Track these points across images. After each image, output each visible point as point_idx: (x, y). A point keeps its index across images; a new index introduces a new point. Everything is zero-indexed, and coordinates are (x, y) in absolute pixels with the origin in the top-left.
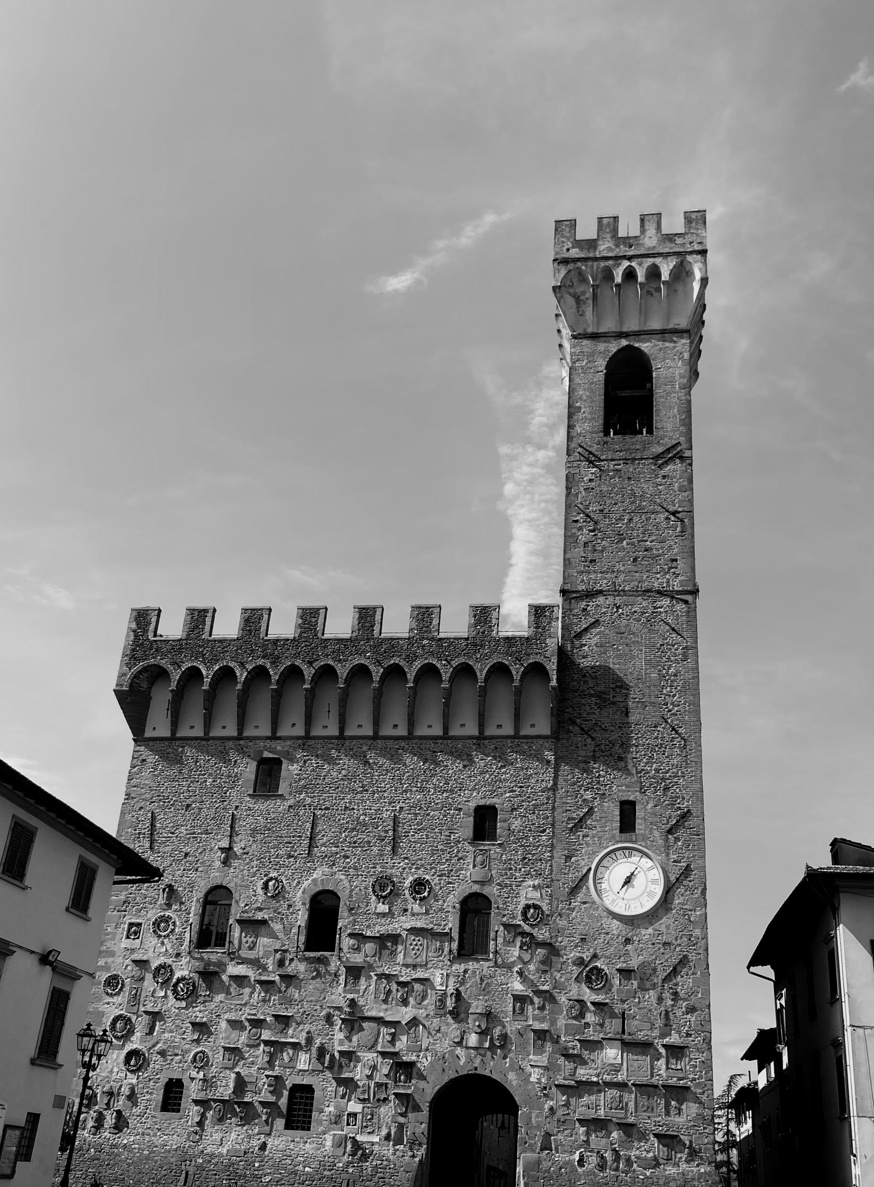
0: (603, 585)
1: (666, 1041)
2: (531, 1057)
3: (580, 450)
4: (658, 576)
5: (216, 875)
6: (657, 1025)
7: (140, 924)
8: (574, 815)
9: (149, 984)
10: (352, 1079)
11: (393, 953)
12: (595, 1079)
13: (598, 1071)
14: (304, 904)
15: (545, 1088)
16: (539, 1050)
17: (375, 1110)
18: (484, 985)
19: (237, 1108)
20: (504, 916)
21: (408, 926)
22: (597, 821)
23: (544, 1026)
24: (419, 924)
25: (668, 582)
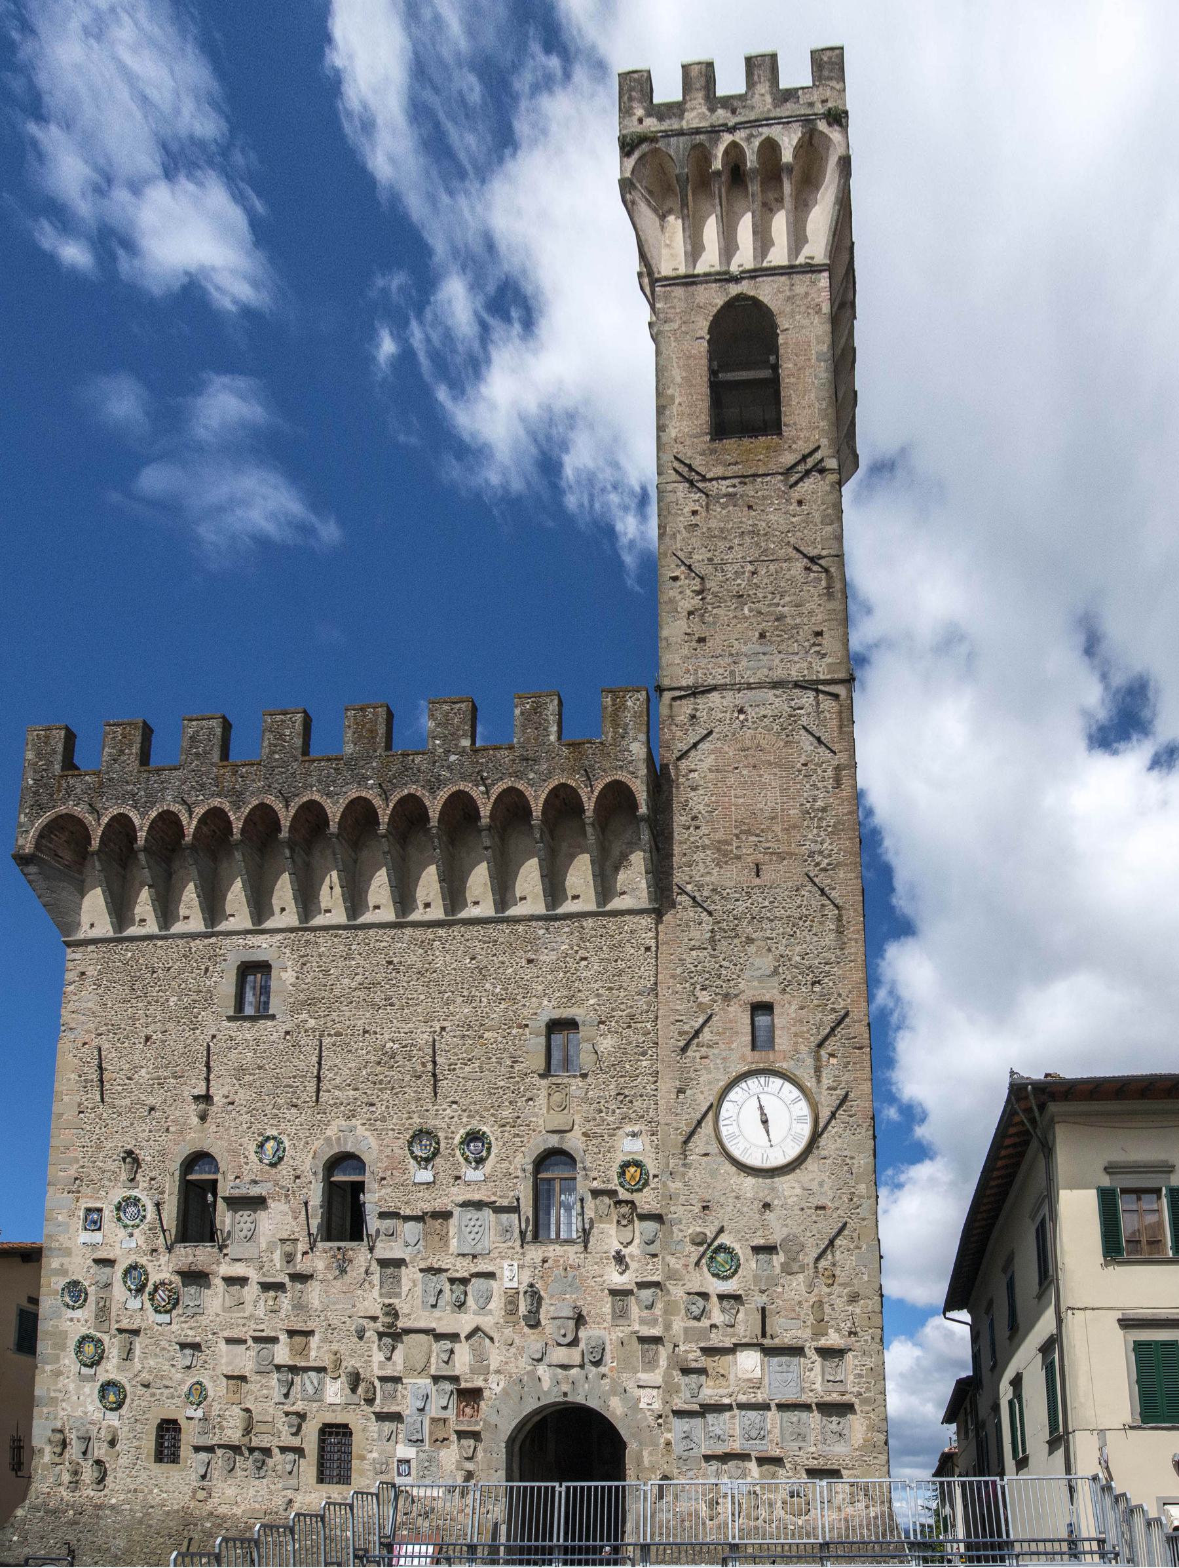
0: (718, 676)
1: (823, 1342)
2: (639, 1375)
3: (676, 464)
4: (796, 659)
5: (195, 1138)
6: (809, 1323)
7: (100, 1210)
8: (686, 1028)
9: (119, 1292)
11: (444, 1238)
12: (726, 1401)
13: (731, 1390)
14: (315, 1174)
15: (660, 1416)
16: (650, 1364)
19: (249, 1452)
20: (595, 1179)
21: (460, 1199)
22: (719, 1034)
23: (655, 1332)
24: (476, 1197)
25: (810, 668)
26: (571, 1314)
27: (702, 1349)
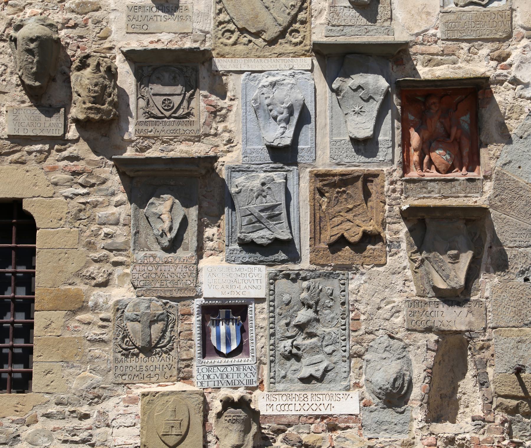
10: (210, 161)
17: (330, 285)
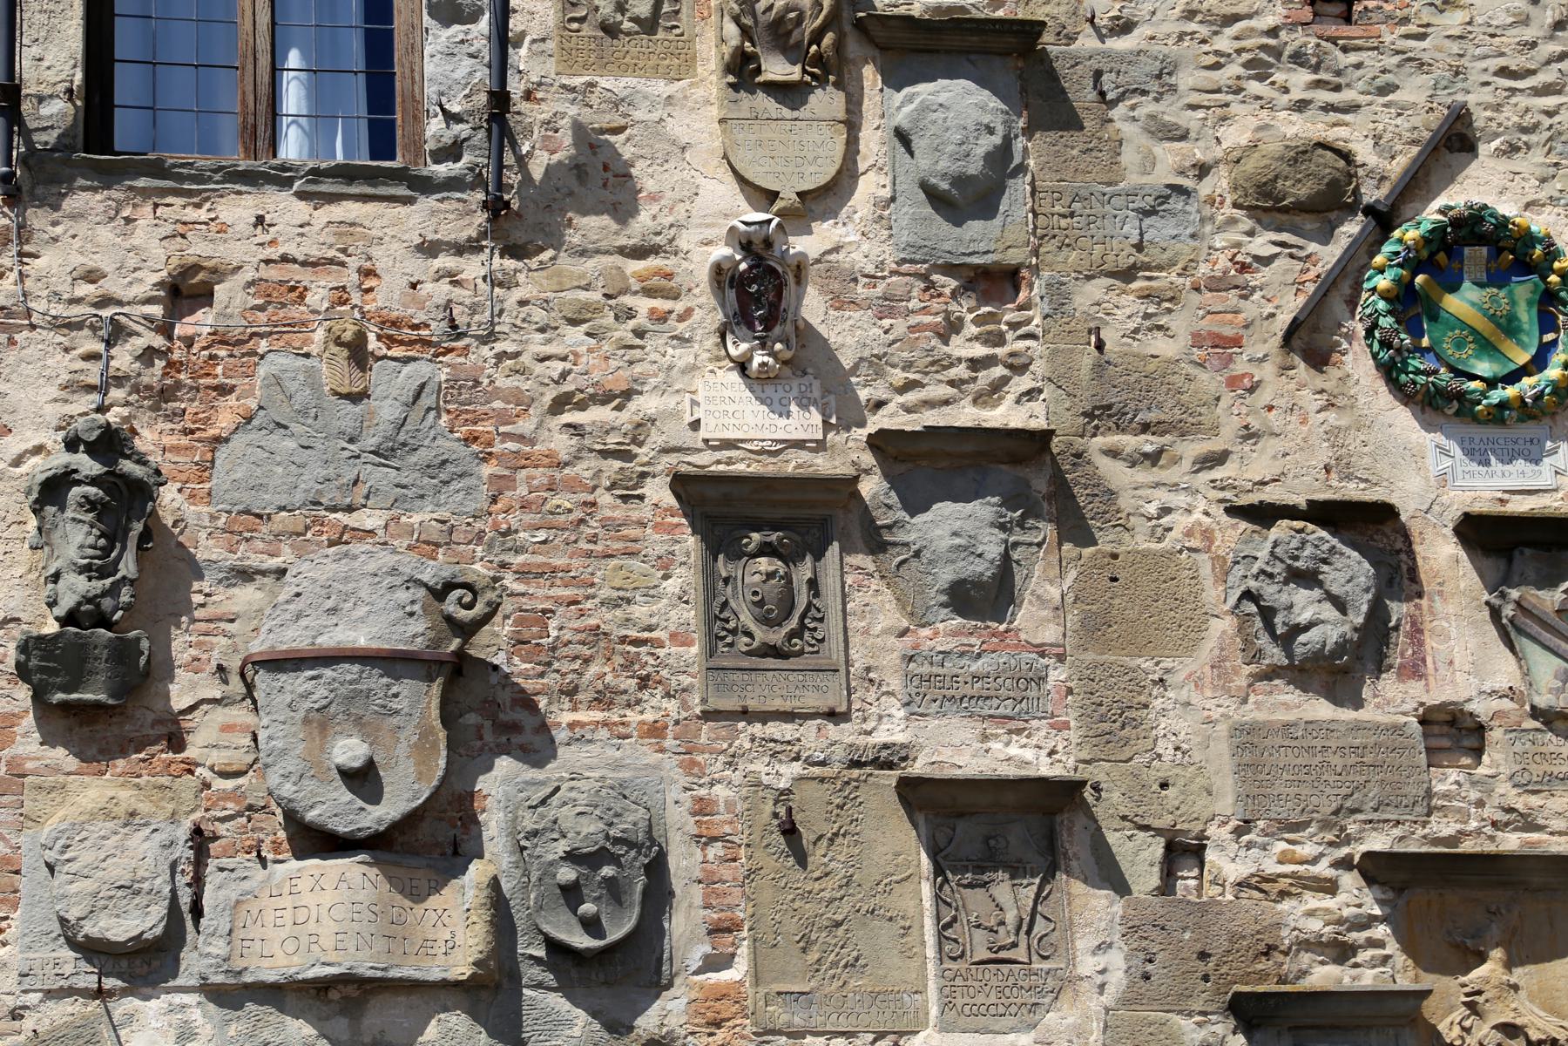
18: (386, 410)
26: (412, 634)
27: (1375, 869)
